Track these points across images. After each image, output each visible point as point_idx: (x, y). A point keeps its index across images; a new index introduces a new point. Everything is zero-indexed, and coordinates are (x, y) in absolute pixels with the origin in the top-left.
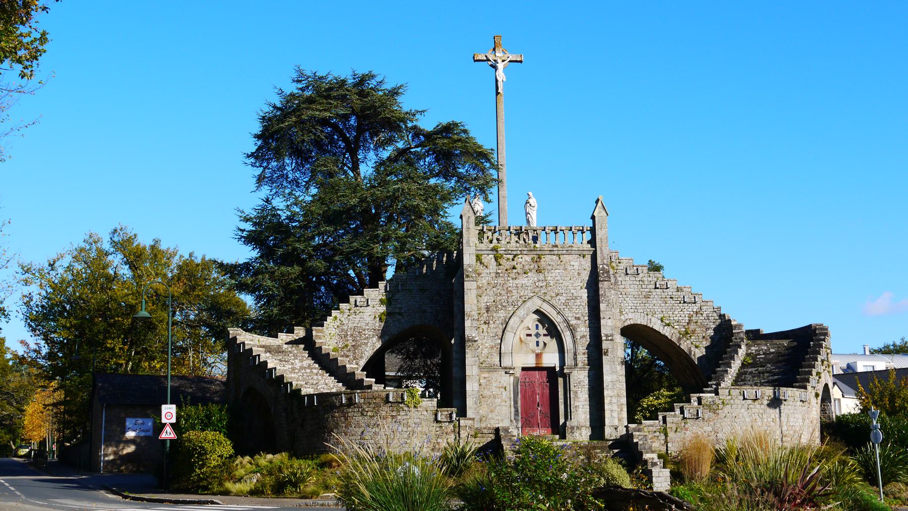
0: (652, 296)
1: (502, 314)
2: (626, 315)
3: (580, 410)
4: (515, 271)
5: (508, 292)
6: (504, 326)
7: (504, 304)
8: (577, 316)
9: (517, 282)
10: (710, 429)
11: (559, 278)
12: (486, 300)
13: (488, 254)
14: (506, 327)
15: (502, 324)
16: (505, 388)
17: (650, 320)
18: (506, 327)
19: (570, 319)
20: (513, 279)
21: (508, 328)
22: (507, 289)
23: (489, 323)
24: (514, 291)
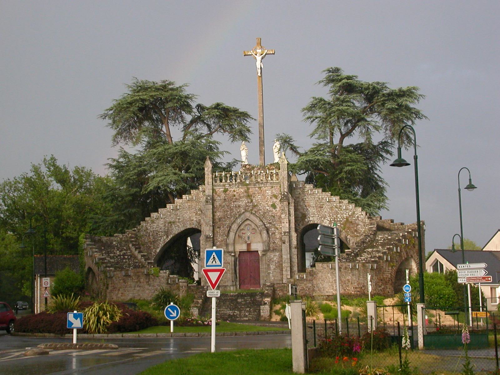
0: (324, 207)
1: (228, 222)
2: (308, 219)
3: (271, 275)
4: (234, 197)
5: (231, 209)
6: (229, 229)
7: (229, 217)
8: (270, 222)
9: (235, 203)
10: (310, 285)
11: (260, 201)
12: (218, 215)
13: (220, 189)
14: (230, 229)
15: (227, 228)
16: (229, 263)
17: (323, 220)
18: (230, 229)
19: (266, 223)
20: (234, 202)
21: (231, 230)
22: (230, 207)
23: (220, 227)
24: (234, 209)
